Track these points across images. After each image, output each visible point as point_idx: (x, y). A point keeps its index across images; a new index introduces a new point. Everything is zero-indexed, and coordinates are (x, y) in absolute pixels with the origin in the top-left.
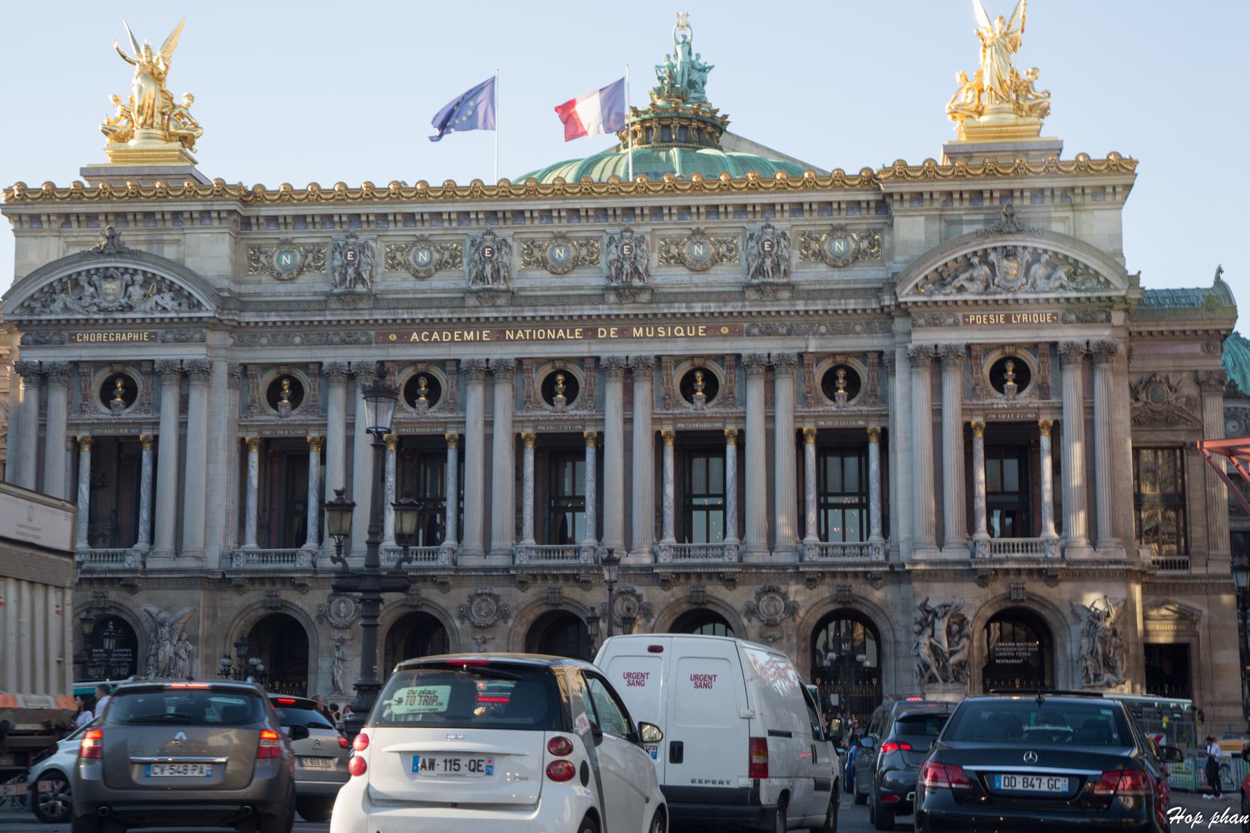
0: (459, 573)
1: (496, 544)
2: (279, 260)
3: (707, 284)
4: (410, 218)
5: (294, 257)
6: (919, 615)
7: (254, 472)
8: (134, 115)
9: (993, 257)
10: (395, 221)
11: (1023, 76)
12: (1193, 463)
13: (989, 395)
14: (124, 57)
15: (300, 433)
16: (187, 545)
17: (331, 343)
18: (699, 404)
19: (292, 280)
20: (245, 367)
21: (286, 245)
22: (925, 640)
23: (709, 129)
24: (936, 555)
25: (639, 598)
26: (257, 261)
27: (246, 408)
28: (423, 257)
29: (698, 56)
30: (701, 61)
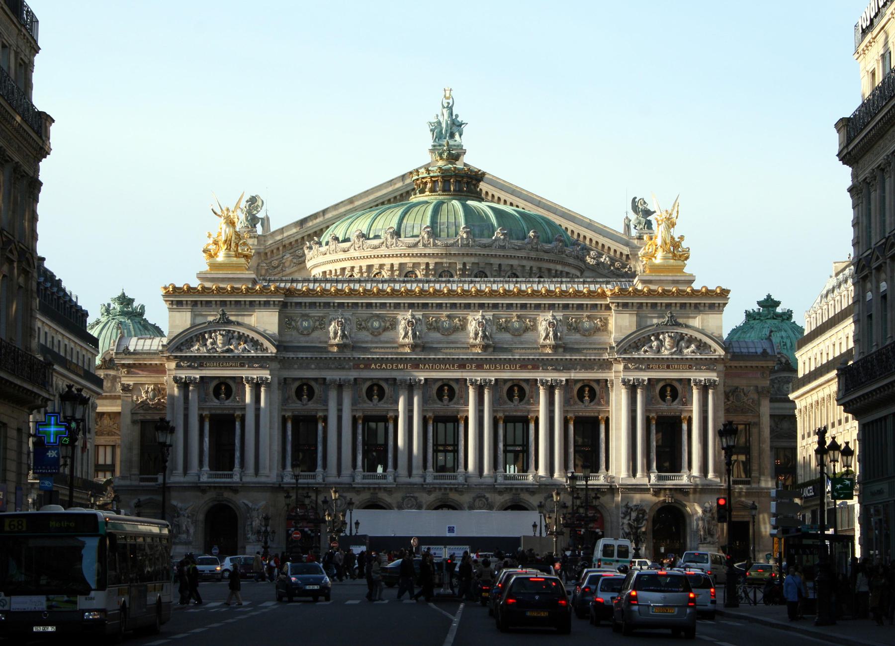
0: (399, 487)
1: (414, 472)
2: (302, 324)
3: (521, 343)
4: (369, 305)
5: (309, 323)
6: (624, 509)
7: (289, 433)
8: (221, 244)
9: (661, 337)
10: (362, 306)
11: (677, 239)
12: (754, 431)
13: (658, 403)
14: (215, 213)
15: (313, 413)
16: (261, 471)
17: (331, 368)
18: (516, 403)
19: (308, 335)
20: (285, 379)
21: (306, 317)
22: (626, 521)
23: (474, 182)
24: (633, 481)
25: (487, 499)
26: (290, 324)
27: (285, 401)
28: (376, 324)
29: (457, 116)
30: (459, 119)
